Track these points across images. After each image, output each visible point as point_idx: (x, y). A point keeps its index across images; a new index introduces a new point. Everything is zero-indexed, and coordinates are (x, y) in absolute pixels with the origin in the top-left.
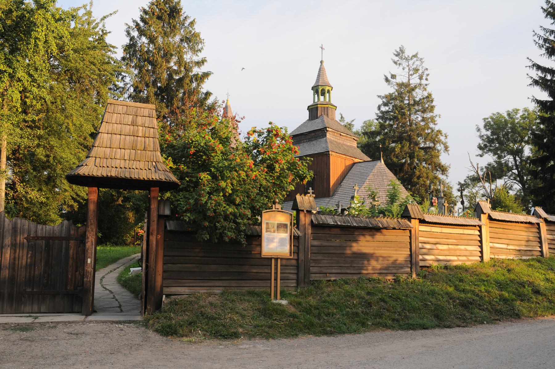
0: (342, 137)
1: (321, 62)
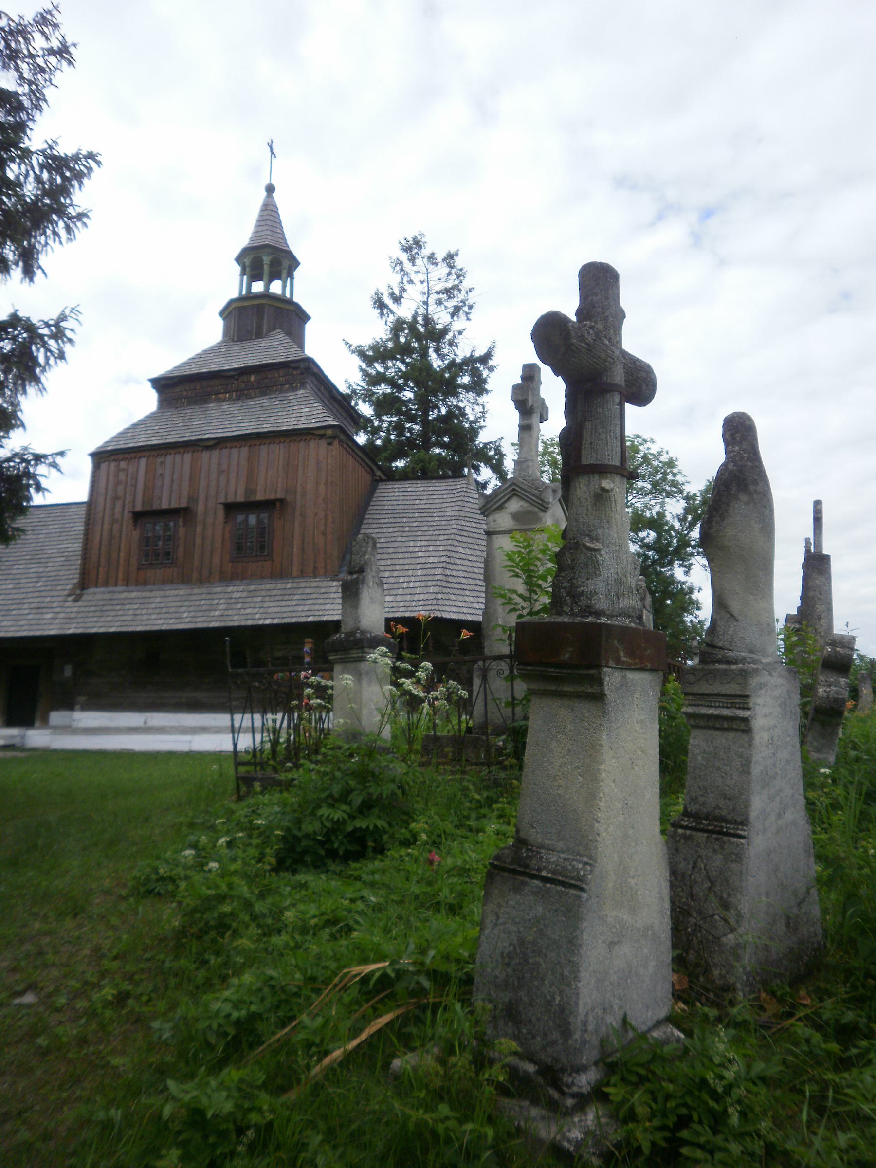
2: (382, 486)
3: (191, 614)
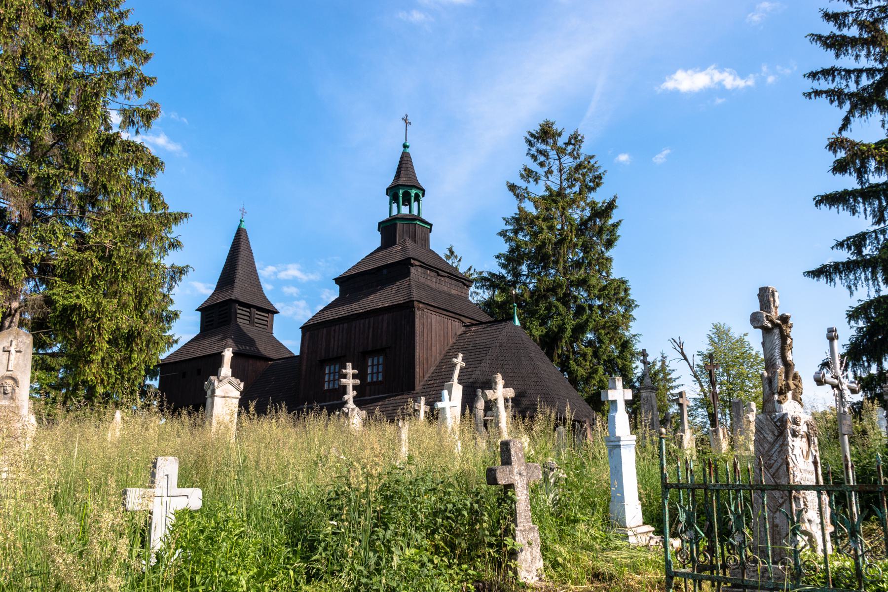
0: (439, 277)
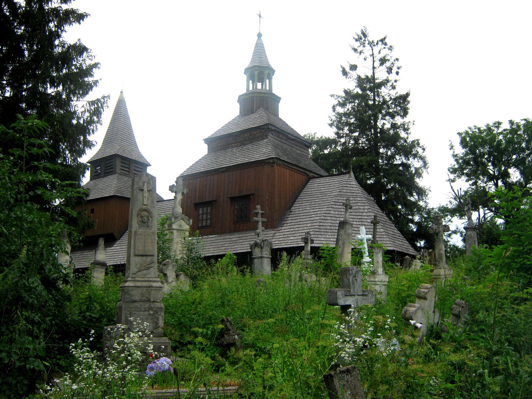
1: (260, 35)
2: (311, 181)
3: (214, 249)
